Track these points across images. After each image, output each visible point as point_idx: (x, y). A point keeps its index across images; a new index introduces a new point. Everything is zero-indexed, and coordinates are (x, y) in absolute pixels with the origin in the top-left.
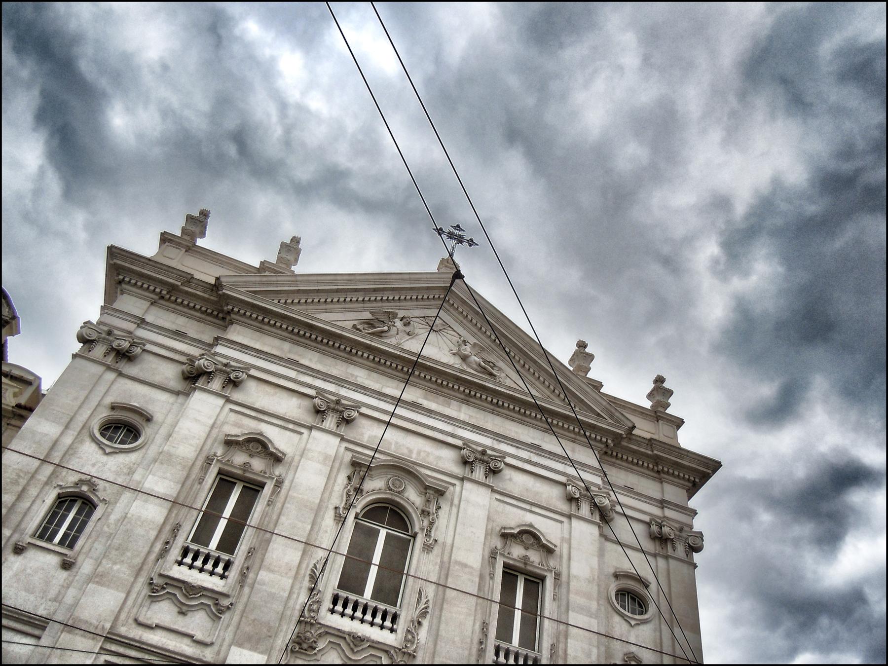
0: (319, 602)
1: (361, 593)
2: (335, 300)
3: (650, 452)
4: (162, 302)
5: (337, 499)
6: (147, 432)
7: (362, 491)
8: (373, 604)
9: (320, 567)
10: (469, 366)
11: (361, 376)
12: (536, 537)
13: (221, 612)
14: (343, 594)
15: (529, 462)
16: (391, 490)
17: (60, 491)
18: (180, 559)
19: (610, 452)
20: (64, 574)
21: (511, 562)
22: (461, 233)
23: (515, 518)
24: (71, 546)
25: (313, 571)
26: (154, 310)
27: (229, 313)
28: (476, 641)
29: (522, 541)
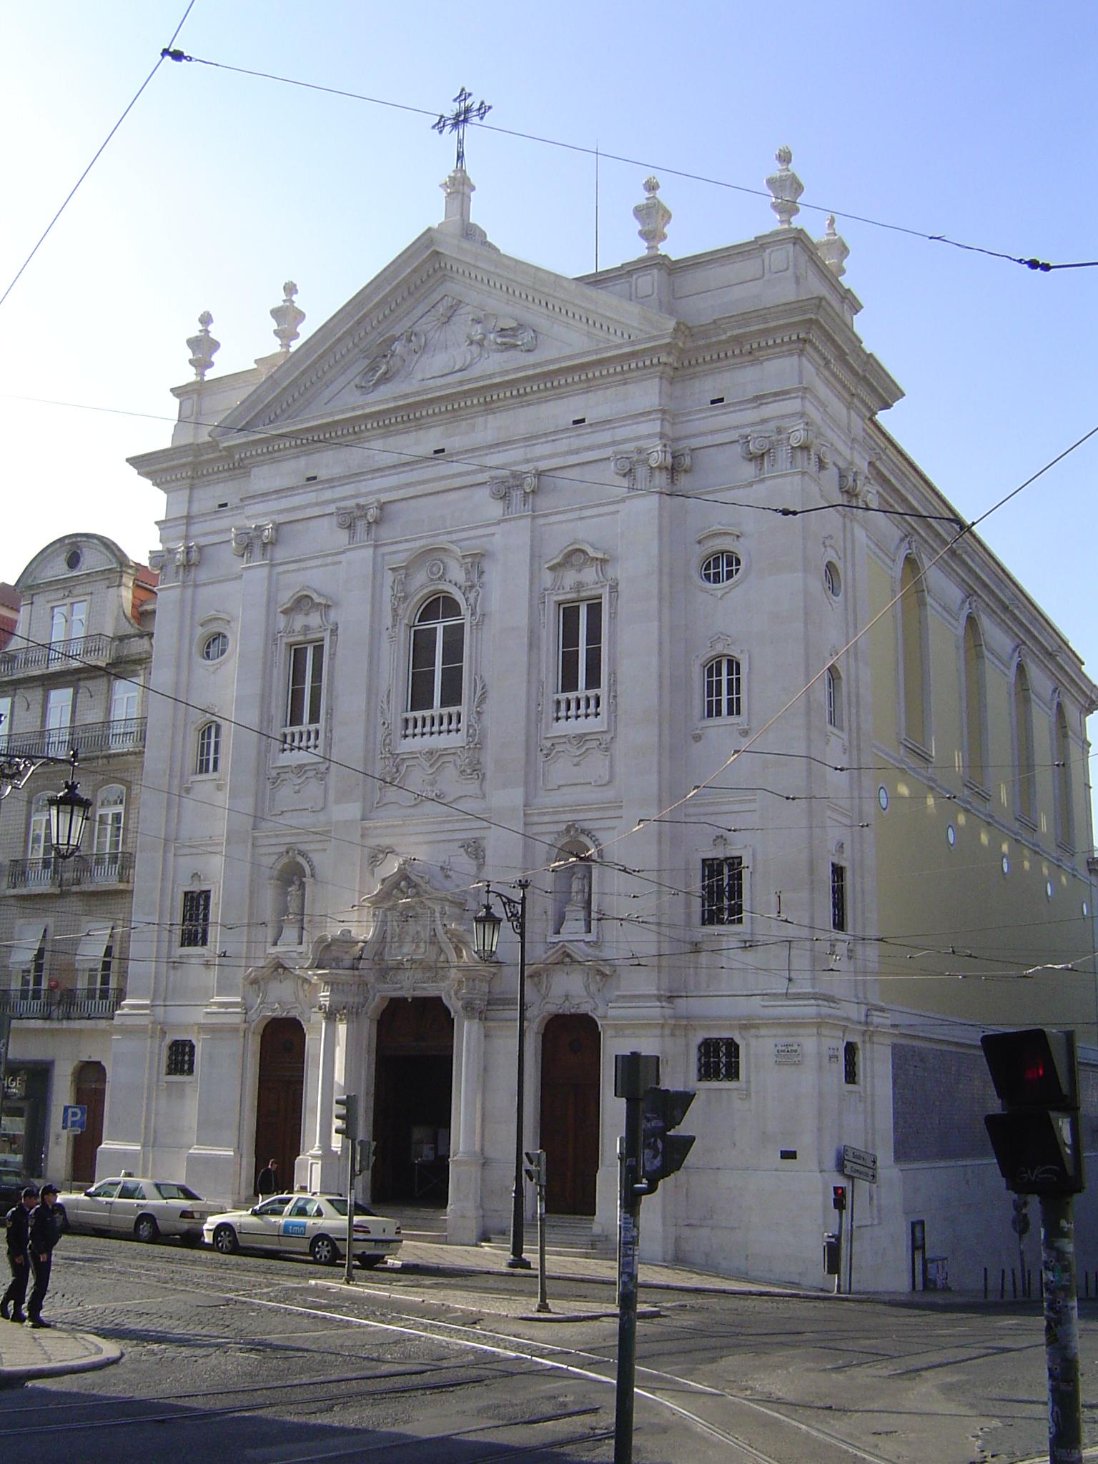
2: (326, 368)
3: (723, 337)
8: (445, 711)
11: (381, 450)
15: (571, 452)
26: (199, 494)
27: (242, 460)
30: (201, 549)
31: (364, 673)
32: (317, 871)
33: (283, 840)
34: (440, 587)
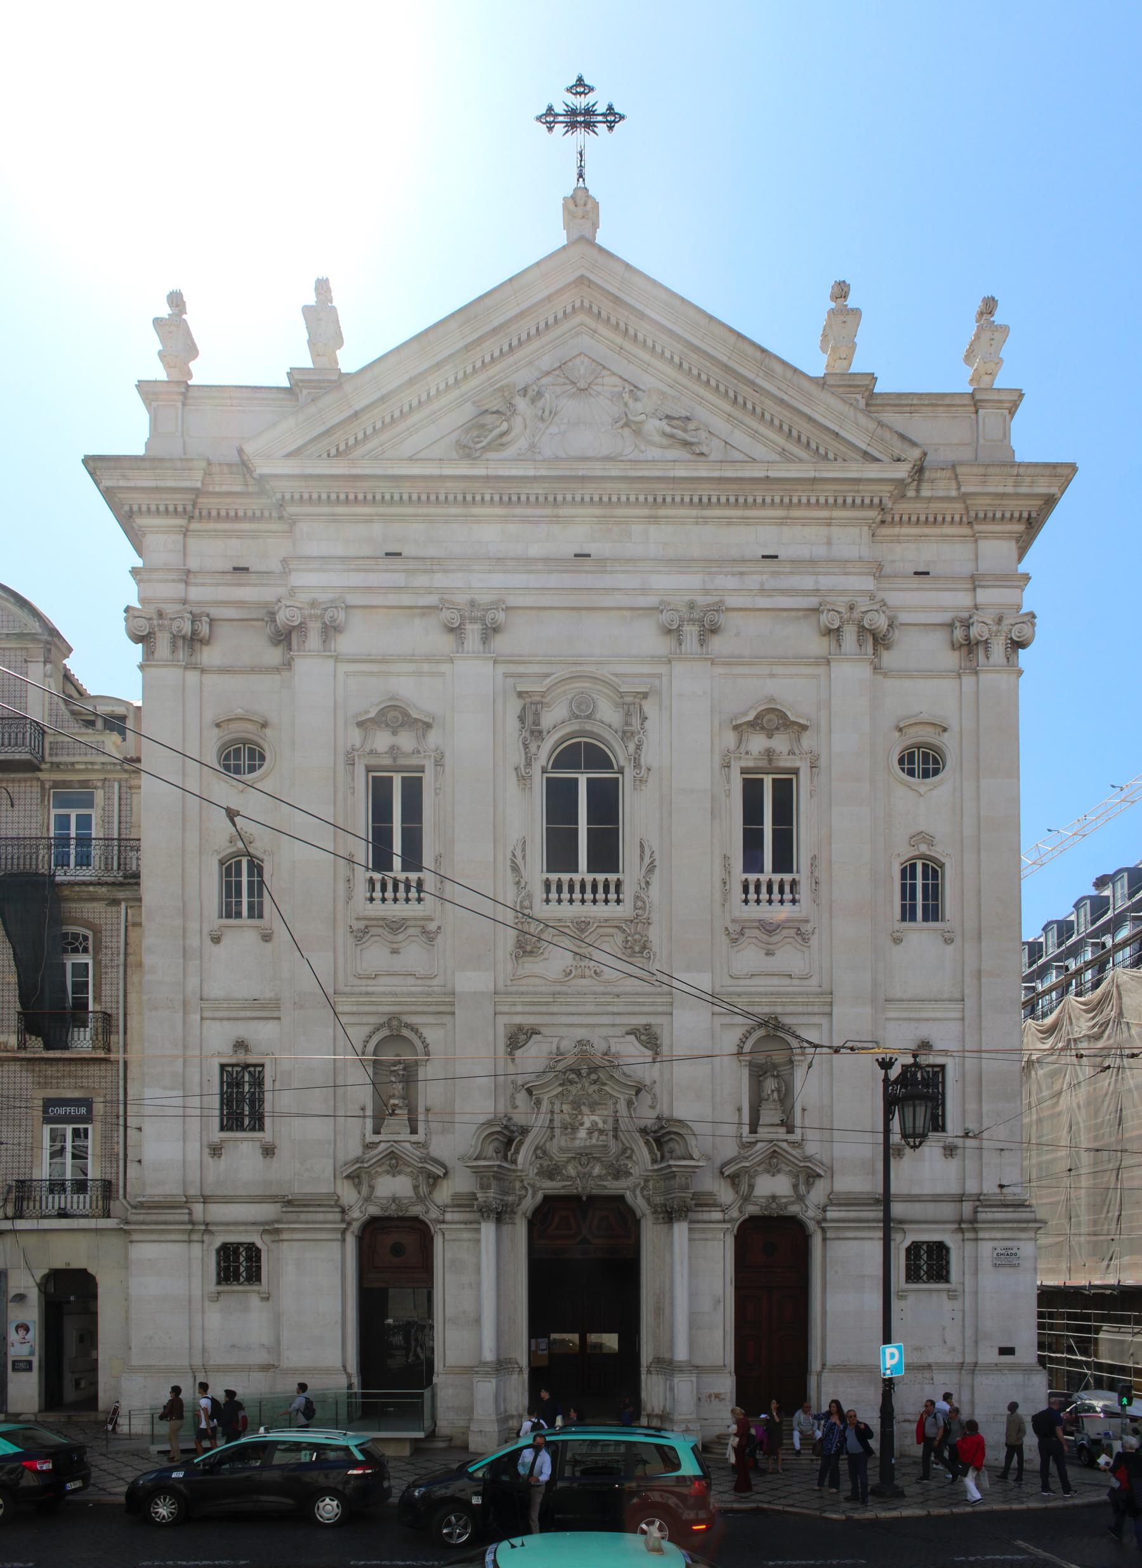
0: (529, 896)
1: (575, 870)
4: (194, 526)
5: (516, 756)
6: (270, 741)
7: (541, 732)
9: (519, 854)
10: (650, 443)
12: (783, 715)
13: (431, 940)
14: (554, 877)
16: (577, 717)
17: (219, 857)
18: (368, 895)
19: (889, 519)
20: (268, 946)
21: (751, 764)
22: (590, 99)
23: (752, 690)
24: (261, 916)
25: (513, 862)
28: (718, 883)
29: (763, 728)
30: (212, 621)
31: (487, 820)
32: (431, 1048)
33: (381, 1009)
34: (588, 727)
